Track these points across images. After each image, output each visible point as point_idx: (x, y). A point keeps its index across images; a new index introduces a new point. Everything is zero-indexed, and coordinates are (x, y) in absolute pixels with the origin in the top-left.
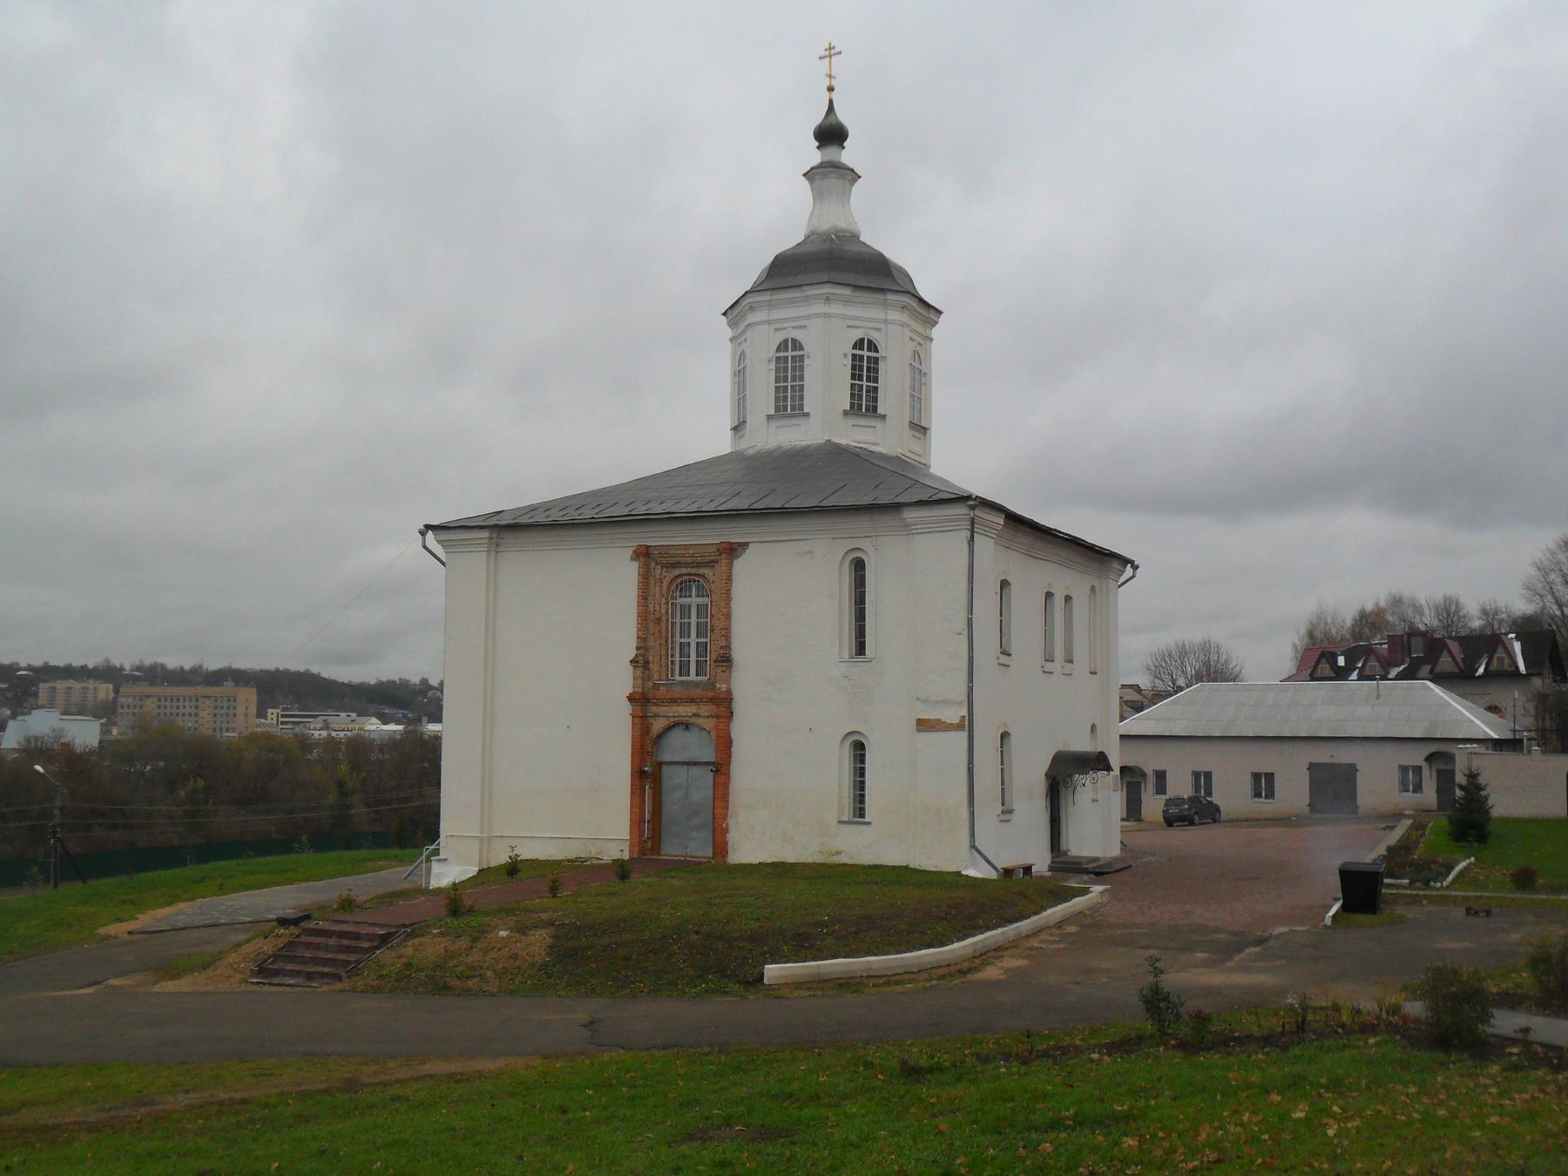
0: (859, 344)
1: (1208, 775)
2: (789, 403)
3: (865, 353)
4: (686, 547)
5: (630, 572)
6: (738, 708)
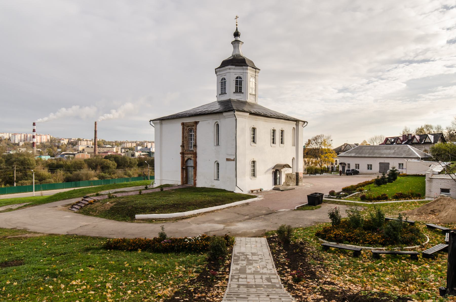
0: (237, 78)
1: (358, 165)
2: (223, 91)
3: (239, 80)
4: (189, 123)
5: (181, 127)
6: (198, 155)
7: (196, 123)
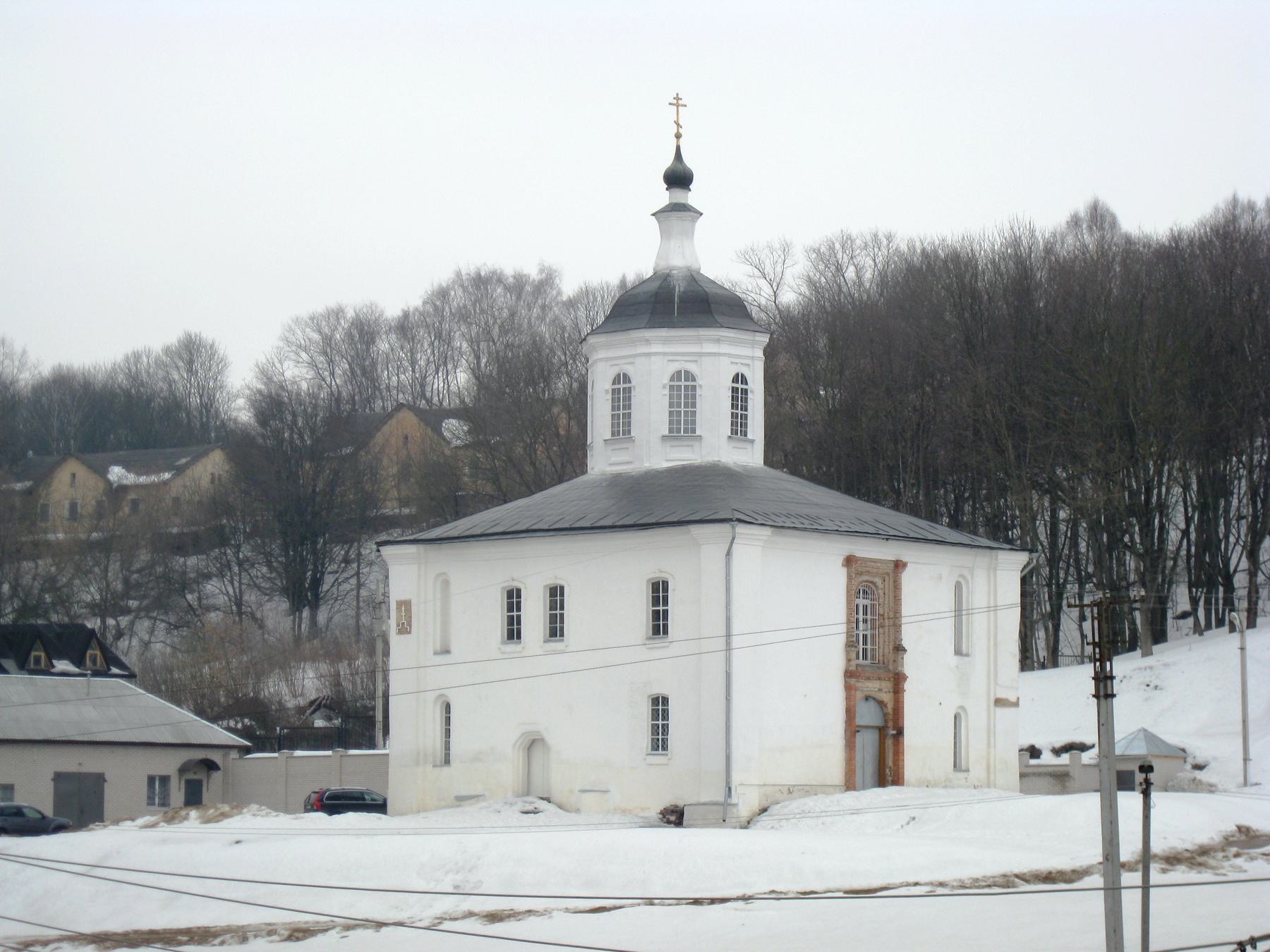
4: (874, 561)
7: (899, 566)
